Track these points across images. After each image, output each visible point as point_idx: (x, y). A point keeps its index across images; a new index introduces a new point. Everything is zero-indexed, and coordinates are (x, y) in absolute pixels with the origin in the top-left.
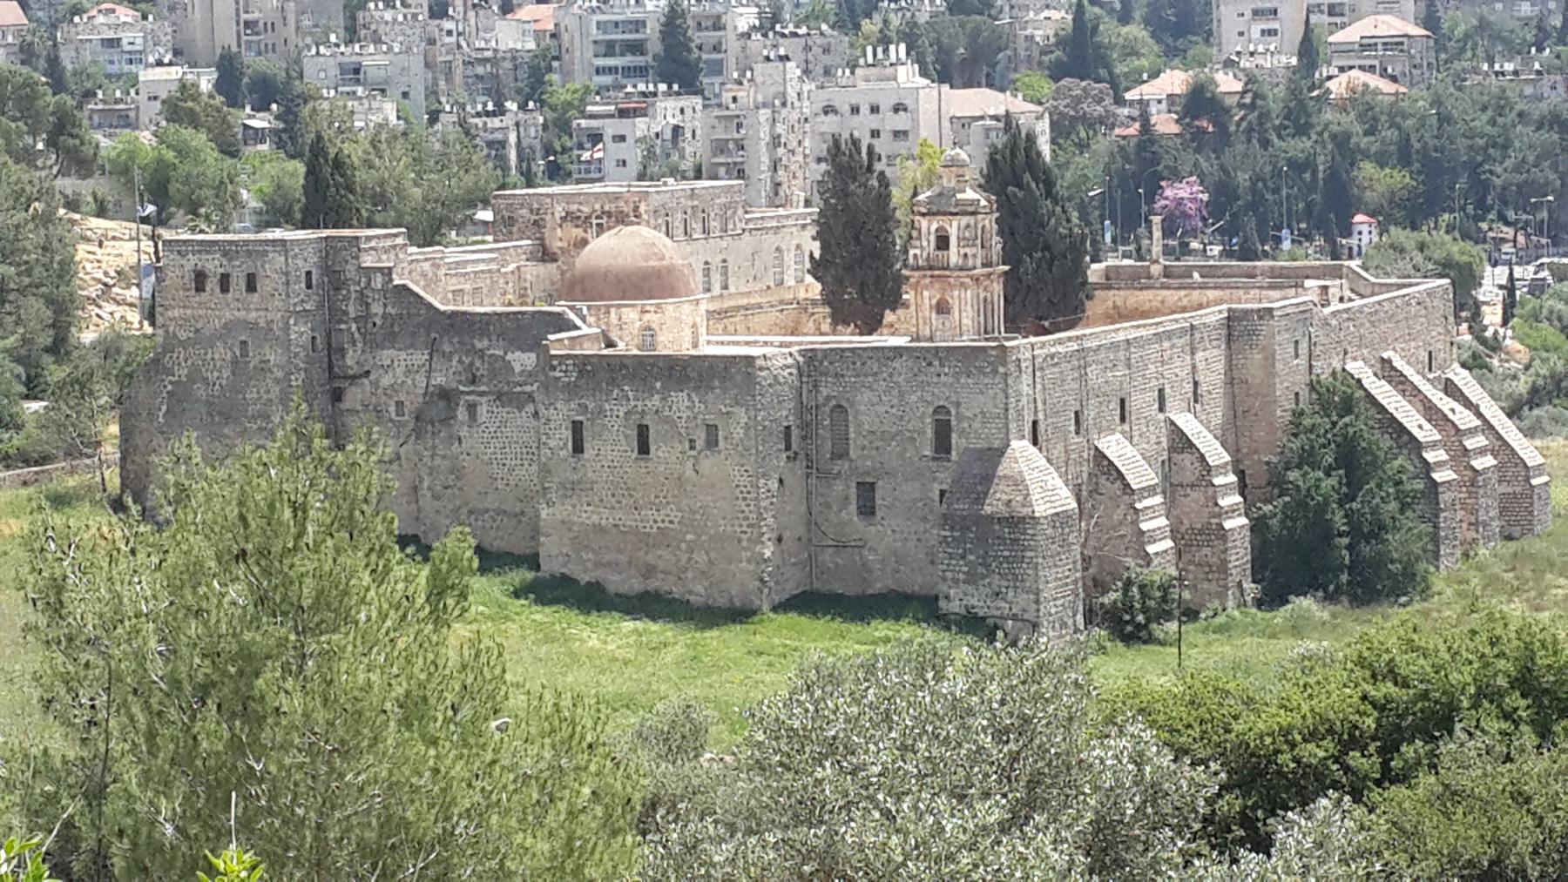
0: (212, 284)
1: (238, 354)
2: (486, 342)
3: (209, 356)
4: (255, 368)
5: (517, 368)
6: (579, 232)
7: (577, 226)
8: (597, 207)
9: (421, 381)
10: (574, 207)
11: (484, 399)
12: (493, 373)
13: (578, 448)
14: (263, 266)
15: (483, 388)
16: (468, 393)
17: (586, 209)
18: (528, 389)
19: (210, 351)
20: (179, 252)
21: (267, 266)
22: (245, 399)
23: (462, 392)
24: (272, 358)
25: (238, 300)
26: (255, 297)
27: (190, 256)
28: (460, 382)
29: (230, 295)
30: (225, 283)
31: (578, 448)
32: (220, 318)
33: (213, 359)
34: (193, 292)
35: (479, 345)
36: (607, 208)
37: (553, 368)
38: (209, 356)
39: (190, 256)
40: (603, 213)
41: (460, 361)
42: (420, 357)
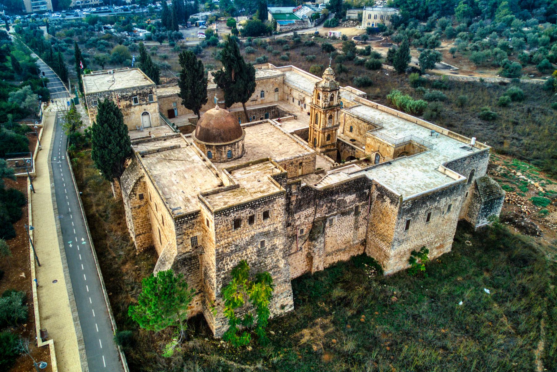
0: (245, 223)
1: (260, 247)
2: (337, 196)
3: (244, 254)
4: (269, 249)
5: (348, 201)
6: (128, 102)
7: (126, 100)
8: (135, 92)
9: (311, 219)
10: (124, 94)
11: (336, 217)
12: (339, 205)
13: (407, 228)
14: (273, 206)
15: (335, 213)
16: (331, 216)
17: (130, 94)
18: (351, 207)
19: (244, 252)
20: (225, 215)
21: (275, 205)
22: (265, 264)
23: (327, 217)
24: (277, 242)
25: (259, 225)
26: (268, 220)
27: (232, 214)
28: (326, 214)
29: (255, 224)
30: (251, 220)
31: (407, 228)
32: (248, 236)
33: (246, 255)
34: (233, 230)
35: (334, 198)
36: (139, 92)
37: (404, 205)
38: (244, 254)
39: (232, 214)
40: (137, 94)
41: (327, 206)
42: (311, 210)
